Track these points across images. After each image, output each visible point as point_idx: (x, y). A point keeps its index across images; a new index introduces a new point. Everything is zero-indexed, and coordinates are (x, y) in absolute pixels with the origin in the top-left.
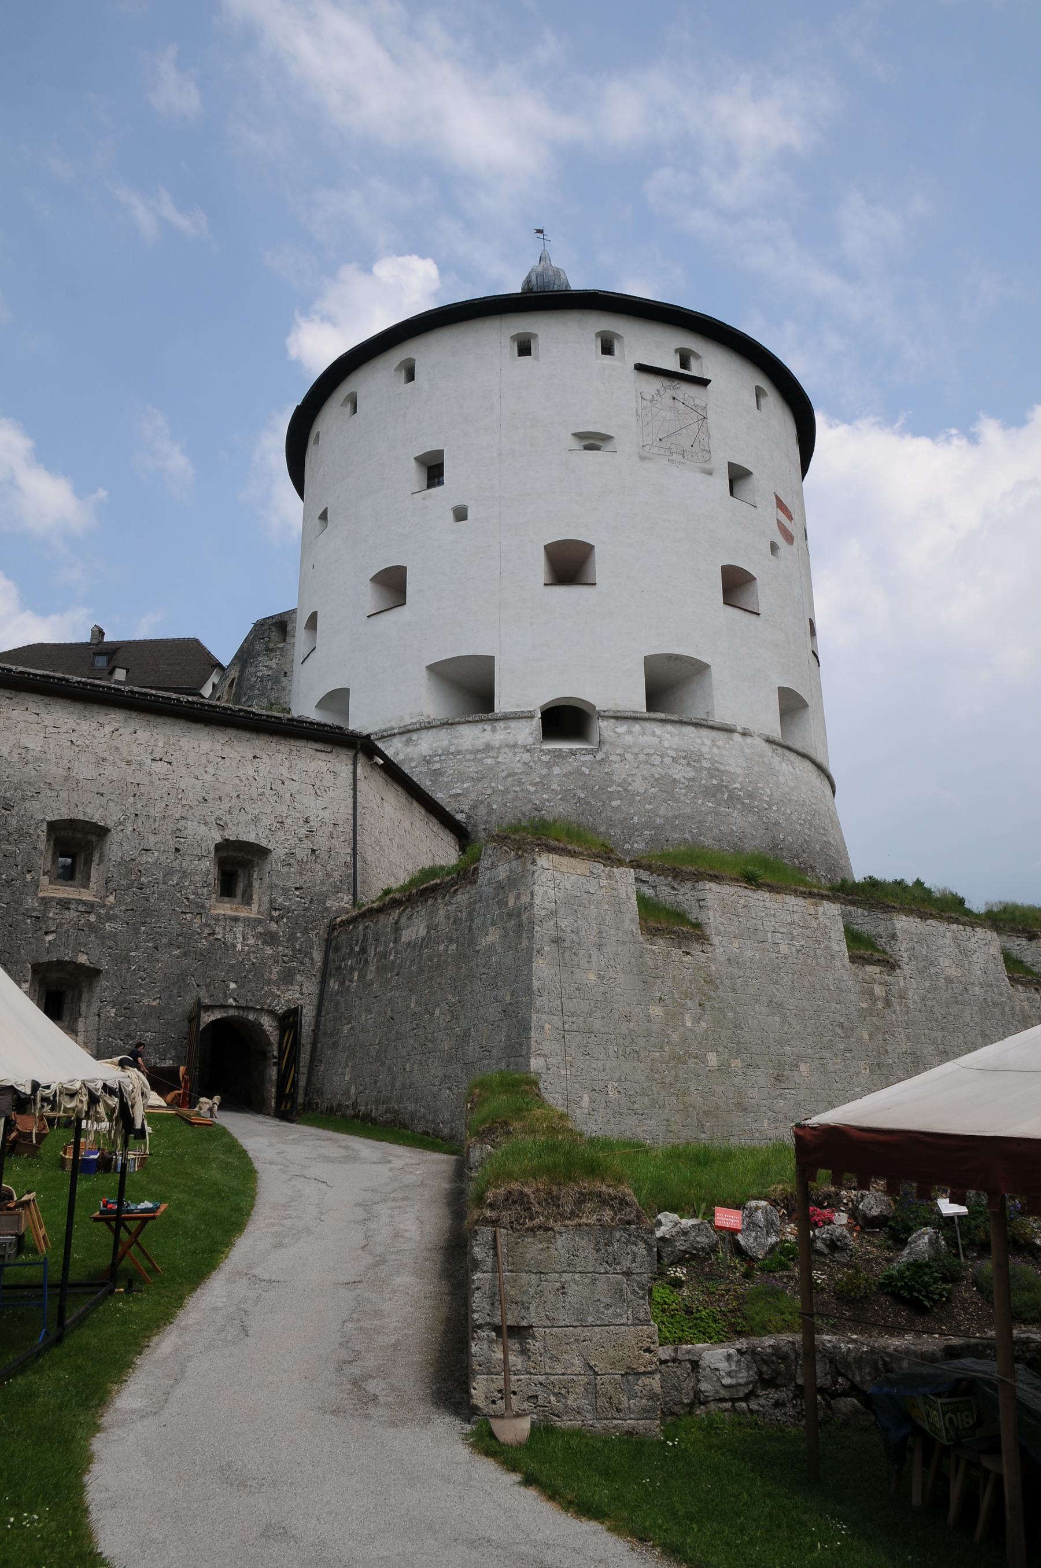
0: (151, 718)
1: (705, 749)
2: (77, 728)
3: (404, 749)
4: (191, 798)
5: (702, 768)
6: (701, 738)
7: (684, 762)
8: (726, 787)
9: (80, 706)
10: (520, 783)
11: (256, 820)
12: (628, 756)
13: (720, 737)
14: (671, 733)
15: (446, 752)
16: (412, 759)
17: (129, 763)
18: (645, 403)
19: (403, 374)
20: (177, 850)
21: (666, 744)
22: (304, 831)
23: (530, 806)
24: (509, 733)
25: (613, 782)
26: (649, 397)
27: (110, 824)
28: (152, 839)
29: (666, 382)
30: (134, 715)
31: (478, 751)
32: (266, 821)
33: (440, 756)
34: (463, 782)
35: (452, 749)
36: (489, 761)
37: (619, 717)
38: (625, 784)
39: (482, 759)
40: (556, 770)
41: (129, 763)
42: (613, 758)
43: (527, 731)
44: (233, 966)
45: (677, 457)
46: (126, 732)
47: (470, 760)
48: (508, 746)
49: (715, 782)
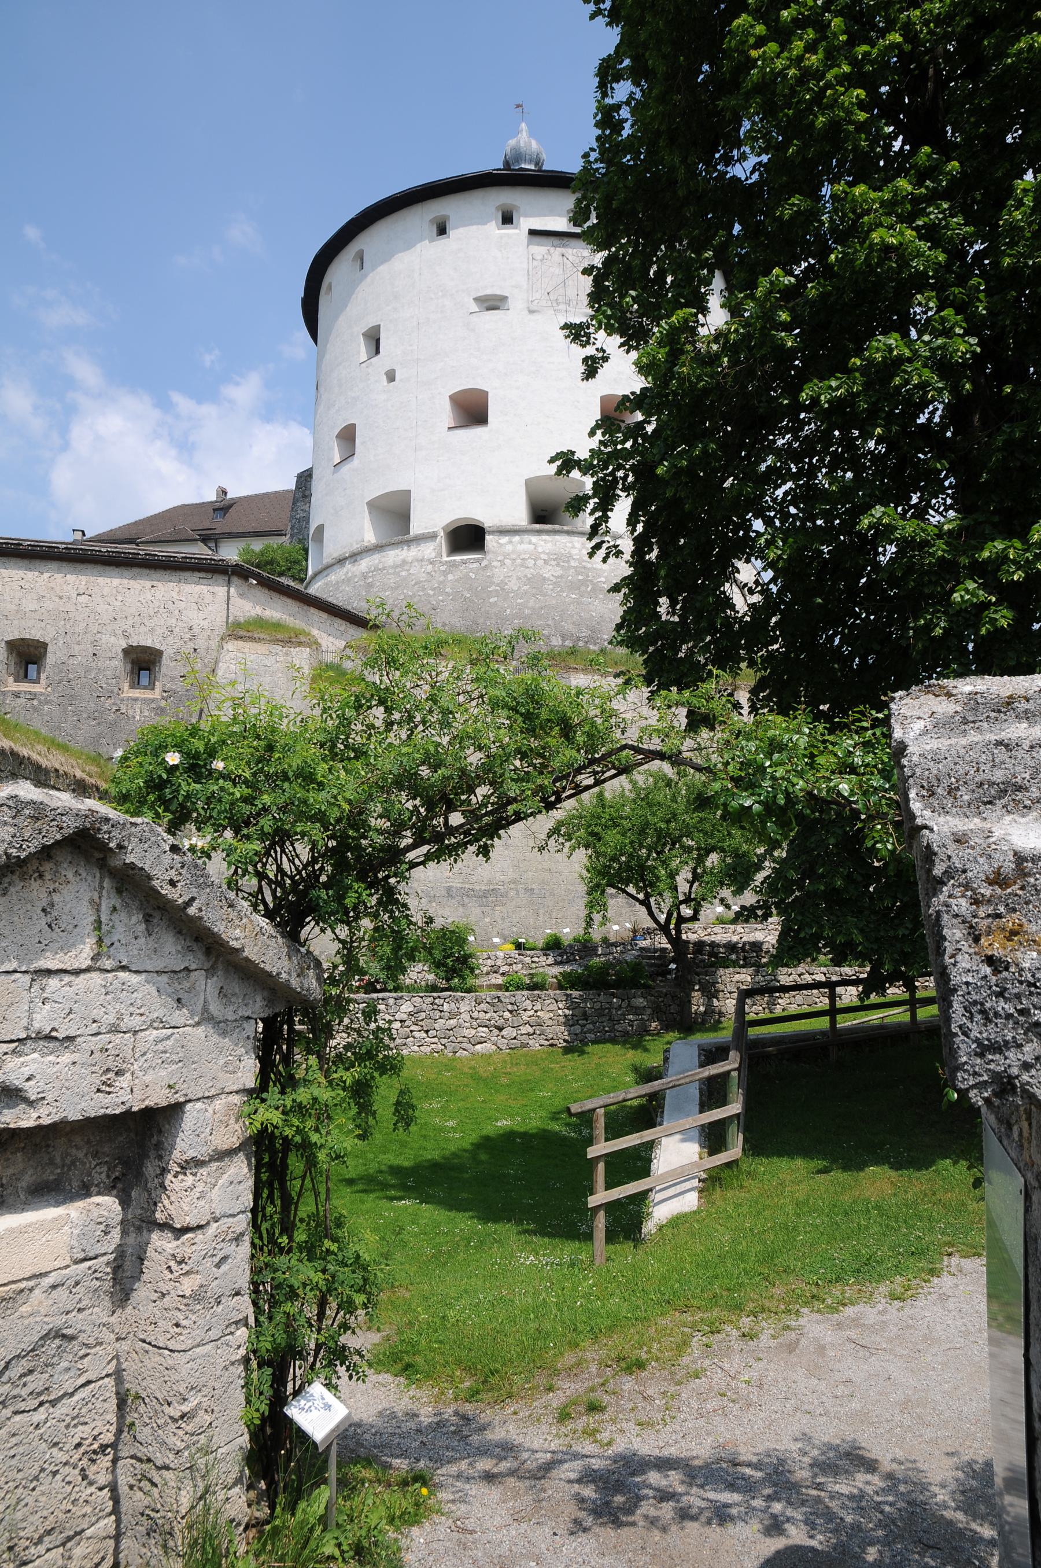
0: (77, 565)
1: (574, 552)
2: (24, 576)
4: (105, 618)
5: (570, 567)
6: (572, 542)
7: (553, 563)
8: (591, 581)
9: (26, 562)
10: (424, 589)
11: (152, 630)
12: (507, 561)
14: (545, 541)
15: (377, 569)
17: (61, 598)
18: (535, 263)
20: (95, 655)
21: (540, 550)
22: (188, 636)
23: (429, 606)
25: (493, 583)
26: (539, 257)
27: (47, 640)
28: (77, 647)
29: (556, 241)
30: (64, 564)
31: (397, 566)
32: (159, 631)
35: (380, 567)
36: (403, 573)
37: (502, 532)
38: (502, 584)
40: (450, 577)
41: (61, 598)
42: (495, 564)
43: (432, 547)
44: (132, 731)
45: (562, 307)
46: (59, 577)
48: (417, 560)
49: (580, 577)
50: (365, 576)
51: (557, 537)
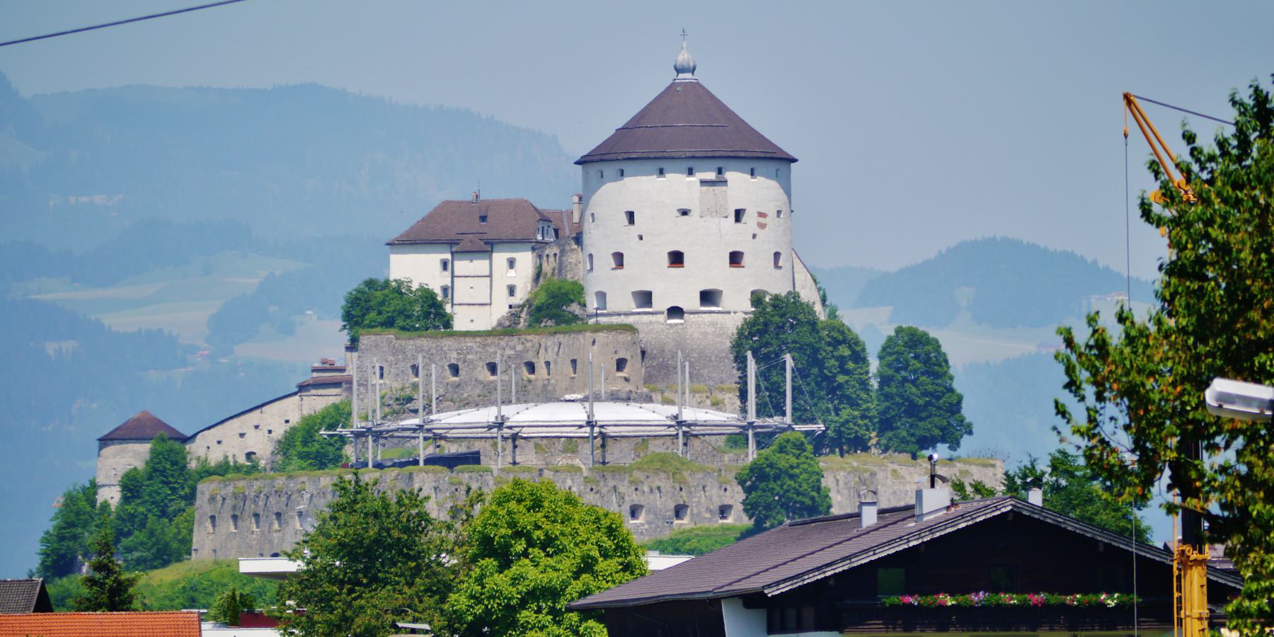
13: (725, 316)
19: (619, 173)
51: (712, 315)
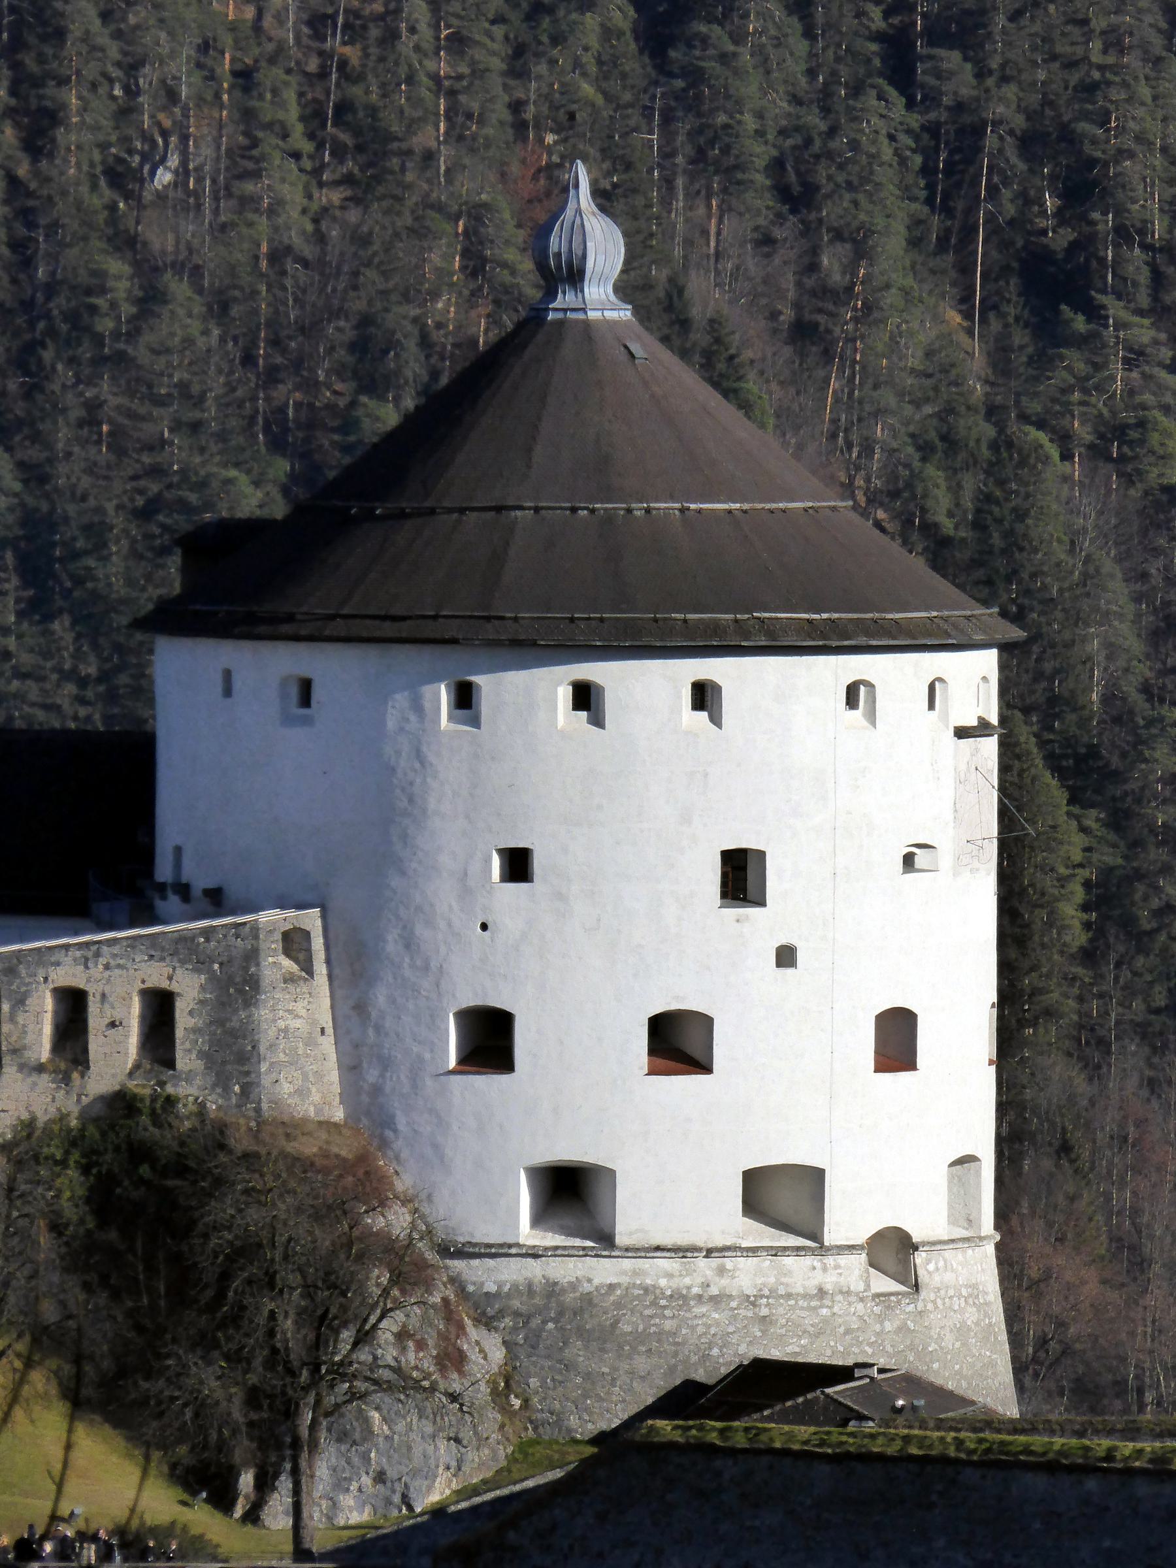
3: (717, 1279)
12: (939, 1302)
16: (730, 1297)
24: (840, 1274)
33: (768, 1297)
34: (800, 1337)
35: (782, 1291)
39: (815, 1308)
40: (888, 1326)
42: (930, 1306)
47: (802, 1308)
50: (751, 1301)
